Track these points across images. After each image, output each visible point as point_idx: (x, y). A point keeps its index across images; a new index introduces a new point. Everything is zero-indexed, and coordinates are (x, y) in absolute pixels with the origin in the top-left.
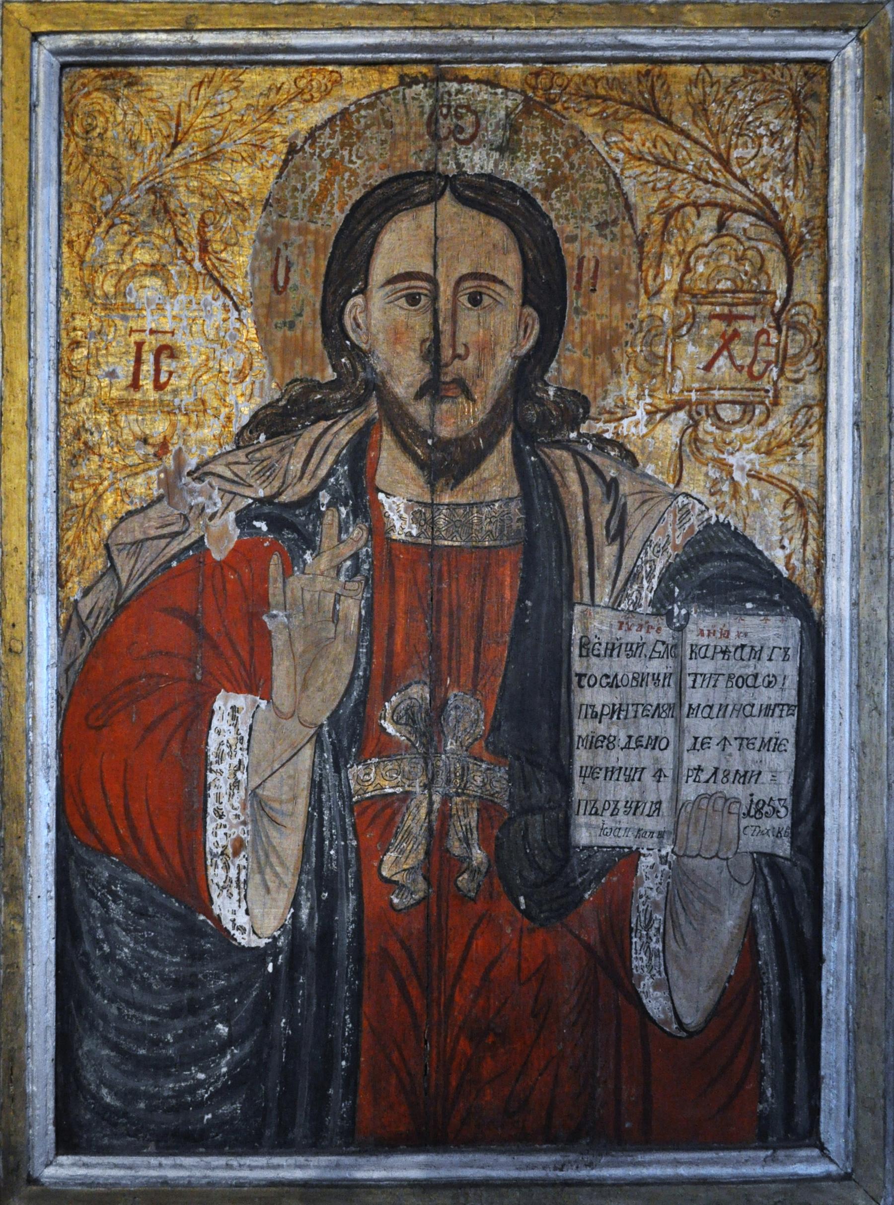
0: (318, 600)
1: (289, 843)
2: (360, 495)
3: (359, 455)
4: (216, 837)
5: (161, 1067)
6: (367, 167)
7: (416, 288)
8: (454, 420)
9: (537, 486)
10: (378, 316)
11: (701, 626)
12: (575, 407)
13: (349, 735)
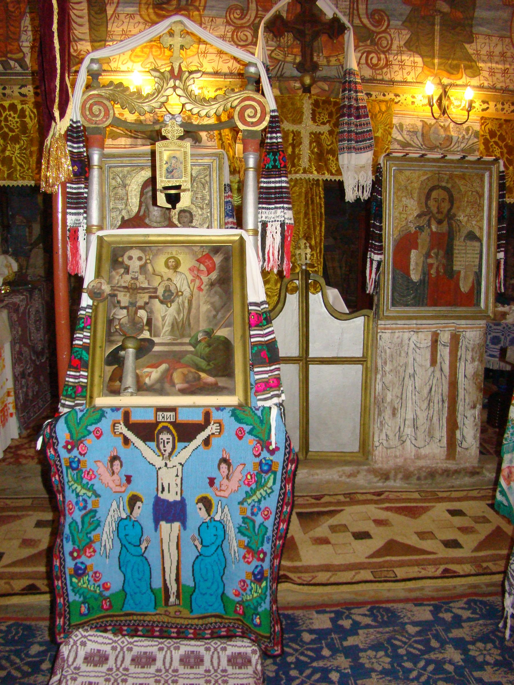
0: (424, 238)
1: (420, 269)
2: (429, 226)
3: (429, 221)
4: (411, 268)
5: (404, 296)
6: (430, 185)
7: (435, 200)
8: (440, 217)
9: (450, 225)
10: (431, 203)
11: (469, 243)
12: (455, 215)
13: (428, 255)
